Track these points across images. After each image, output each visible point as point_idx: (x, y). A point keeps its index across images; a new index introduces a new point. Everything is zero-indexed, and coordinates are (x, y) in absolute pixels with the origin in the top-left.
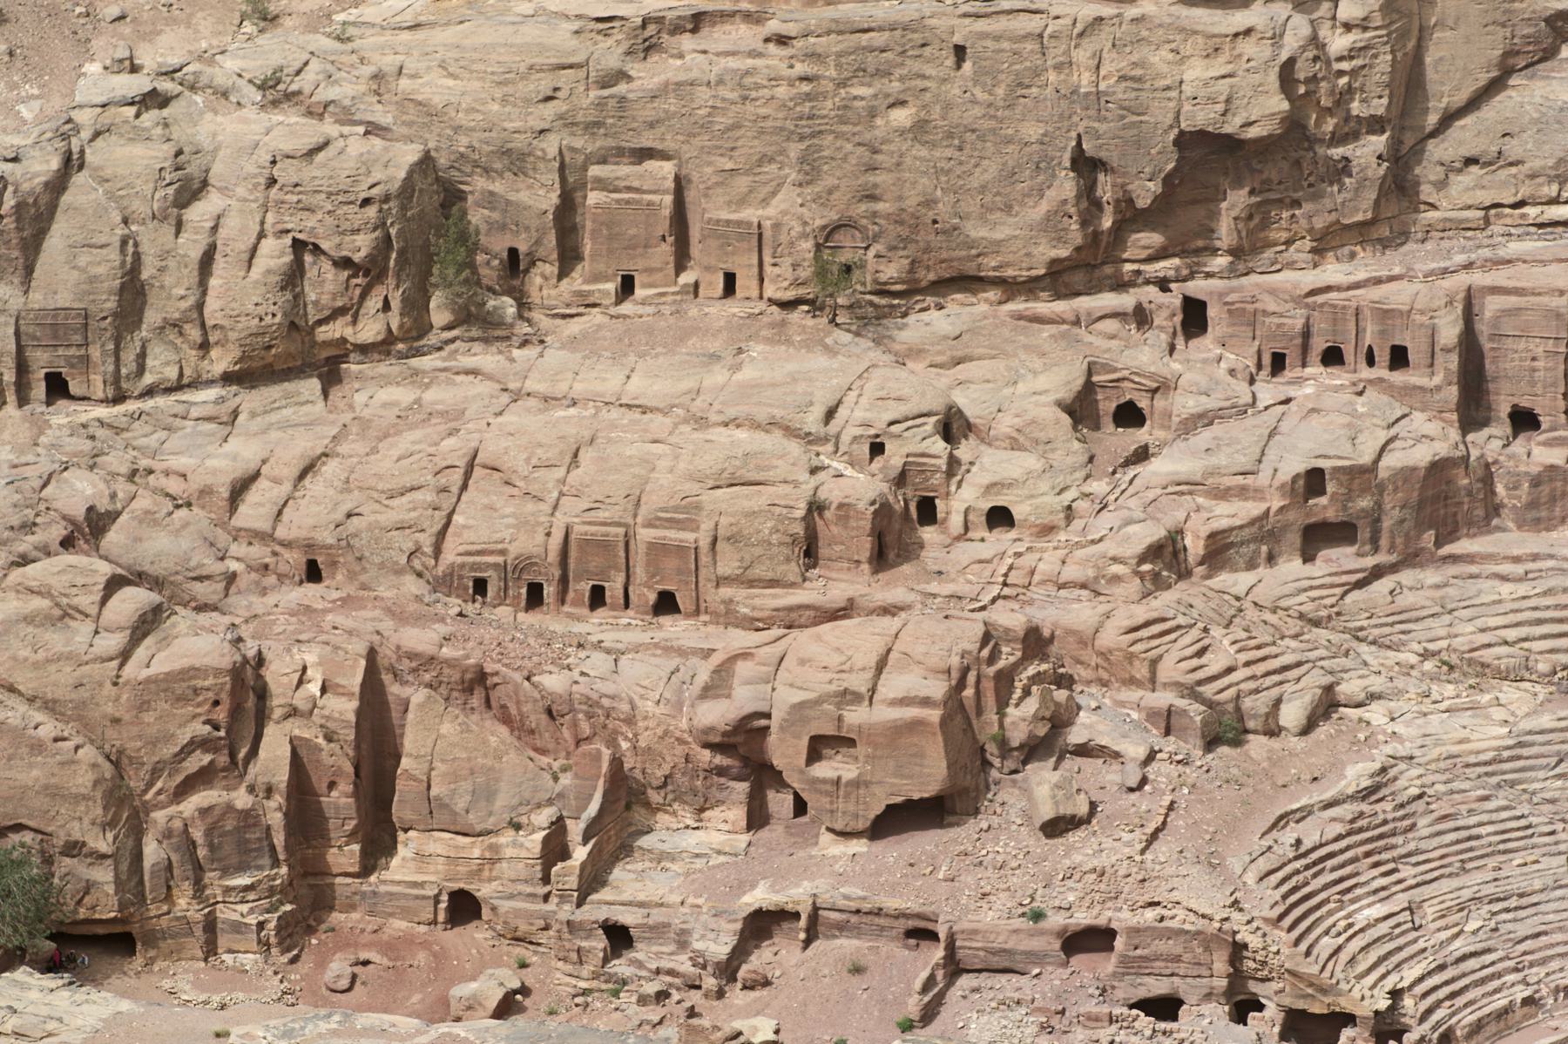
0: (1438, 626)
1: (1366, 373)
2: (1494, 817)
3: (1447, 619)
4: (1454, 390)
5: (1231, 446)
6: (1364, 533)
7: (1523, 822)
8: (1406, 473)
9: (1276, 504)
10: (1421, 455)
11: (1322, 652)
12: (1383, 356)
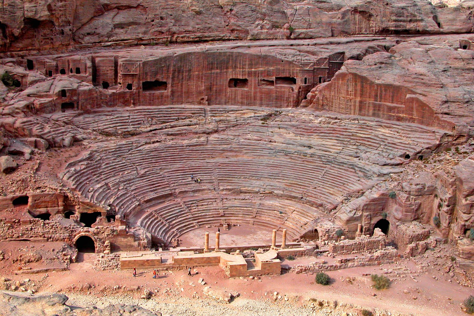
0: (95, 125)
1: (71, 74)
2: (118, 163)
3: (96, 123)
4: (91, 77)
5: (43, 86)
6: (76, 105)
7: (125, 164)
8: (85, 92)
9: (55, 98)
10: (86, 88)
11: (70, 129)
12: (74, 70)
